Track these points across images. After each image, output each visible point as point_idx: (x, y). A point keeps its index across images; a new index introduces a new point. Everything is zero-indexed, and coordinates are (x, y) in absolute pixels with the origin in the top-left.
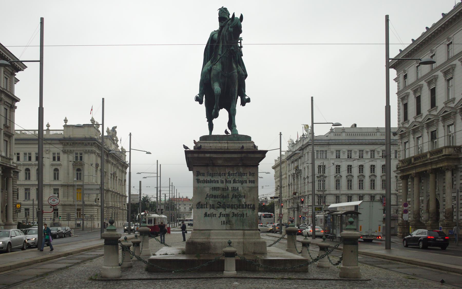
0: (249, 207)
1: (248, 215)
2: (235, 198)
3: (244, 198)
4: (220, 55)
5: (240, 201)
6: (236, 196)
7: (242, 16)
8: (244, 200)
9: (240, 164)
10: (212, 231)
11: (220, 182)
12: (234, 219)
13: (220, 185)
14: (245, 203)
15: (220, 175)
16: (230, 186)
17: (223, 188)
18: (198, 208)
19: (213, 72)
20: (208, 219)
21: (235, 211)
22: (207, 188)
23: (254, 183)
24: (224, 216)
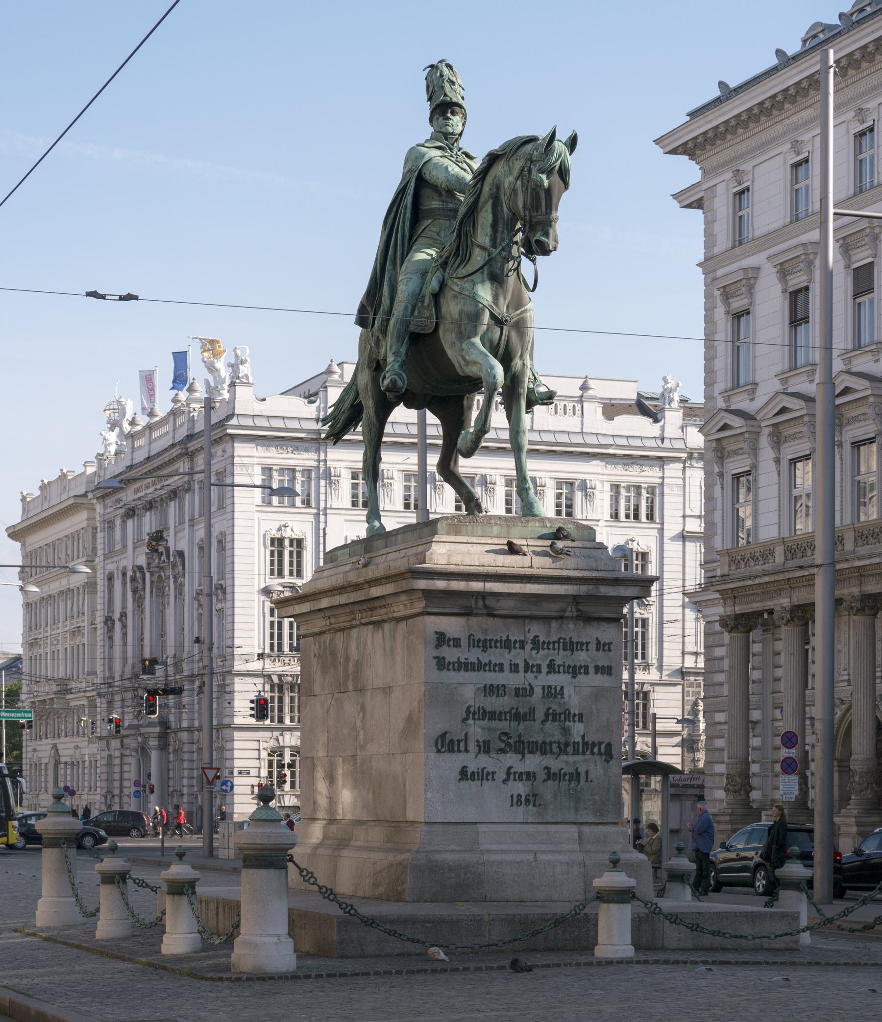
0: (596, 750)
1: (592, 776)
2: (554, 720)
3: (581, 720)
4: (483, 248)
5: (566, 731)
6: (555, 717)
8: (578, 729)
9: (570, 614)
10: (482, 828)
11: (506, 667)
12: (548, 789)
14: (583, 737)
15: (507, 644)
17: (517, 690)
18: (439, 751)
20: (472, 786)
21: (555, 764)
22: (468, 687)
23: (610, 673)
24: (521, 780)
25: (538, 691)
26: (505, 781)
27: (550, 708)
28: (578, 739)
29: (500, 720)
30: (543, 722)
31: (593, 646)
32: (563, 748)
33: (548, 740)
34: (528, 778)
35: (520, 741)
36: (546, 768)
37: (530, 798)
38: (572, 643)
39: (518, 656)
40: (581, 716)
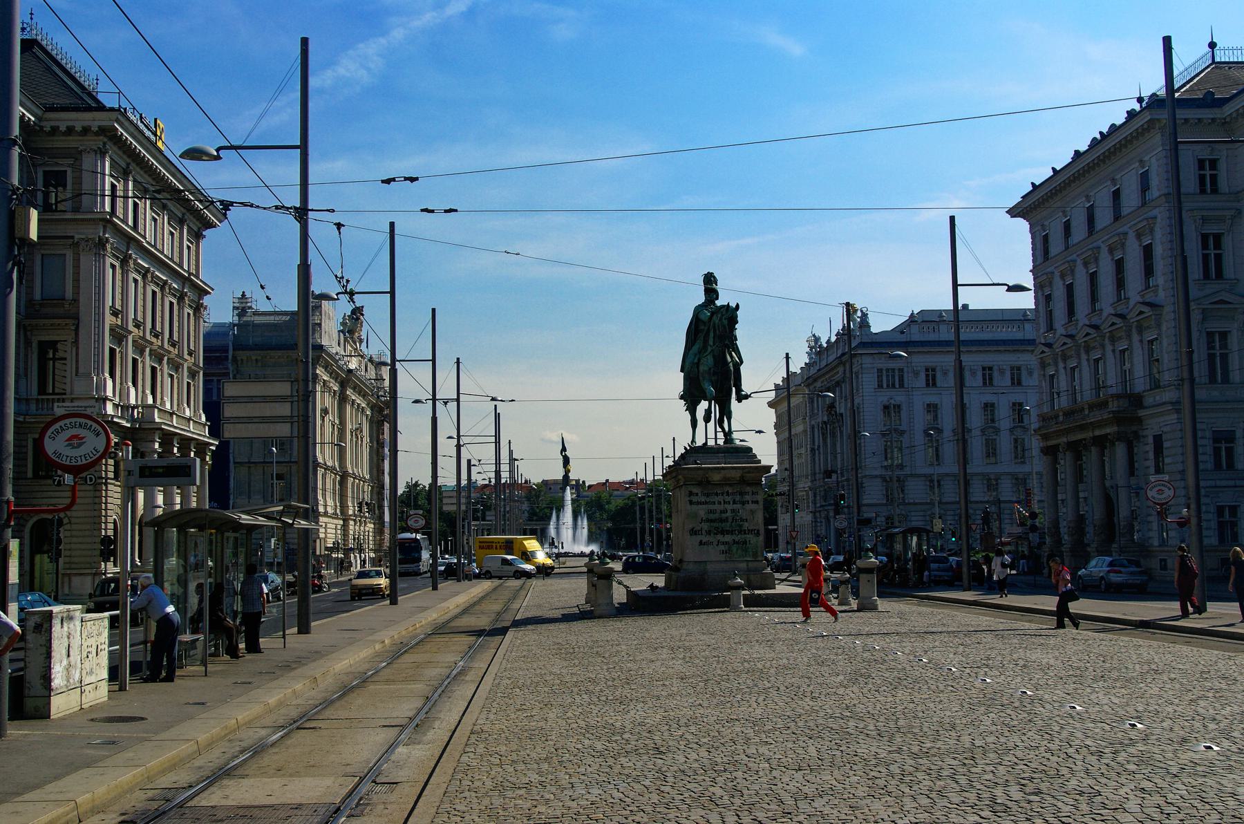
5: (741, 526)
7: (738, 306)
12: (734, 548)
13: (716, 507)
15: (717, 494)
16: (729, 507)
19: (702, 368)
22: (702, 511)
32: (740, 532)
39: (720, 498)
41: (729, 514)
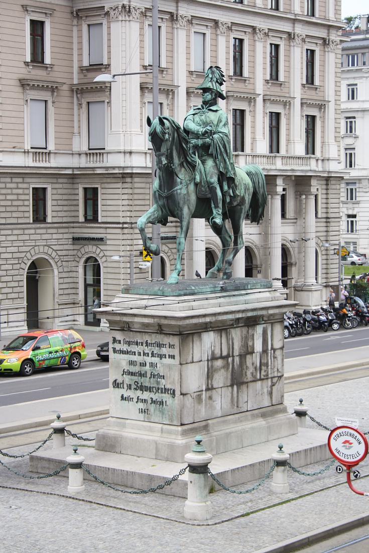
0: (169, 392)
1: (167, 403)
3: (164, 378)
5: (158, 383)
11: (137, 353)
12: (152, 408)
15: (137, 344)
16: (149, 360)
21: (155, 397)
25: (148, 364)
26: (137, 402)
27: (152, 372)
28: (163, 387)
29: (135, 376)
30: (150, 378)
31: (167, 346)
33: (151, 386)
34: (145, 402)
35: (141, 386)
36: (151, 398)
37: (146, 411)
38: (160, 344)
40: (163, 376)
41: (148, 367)
